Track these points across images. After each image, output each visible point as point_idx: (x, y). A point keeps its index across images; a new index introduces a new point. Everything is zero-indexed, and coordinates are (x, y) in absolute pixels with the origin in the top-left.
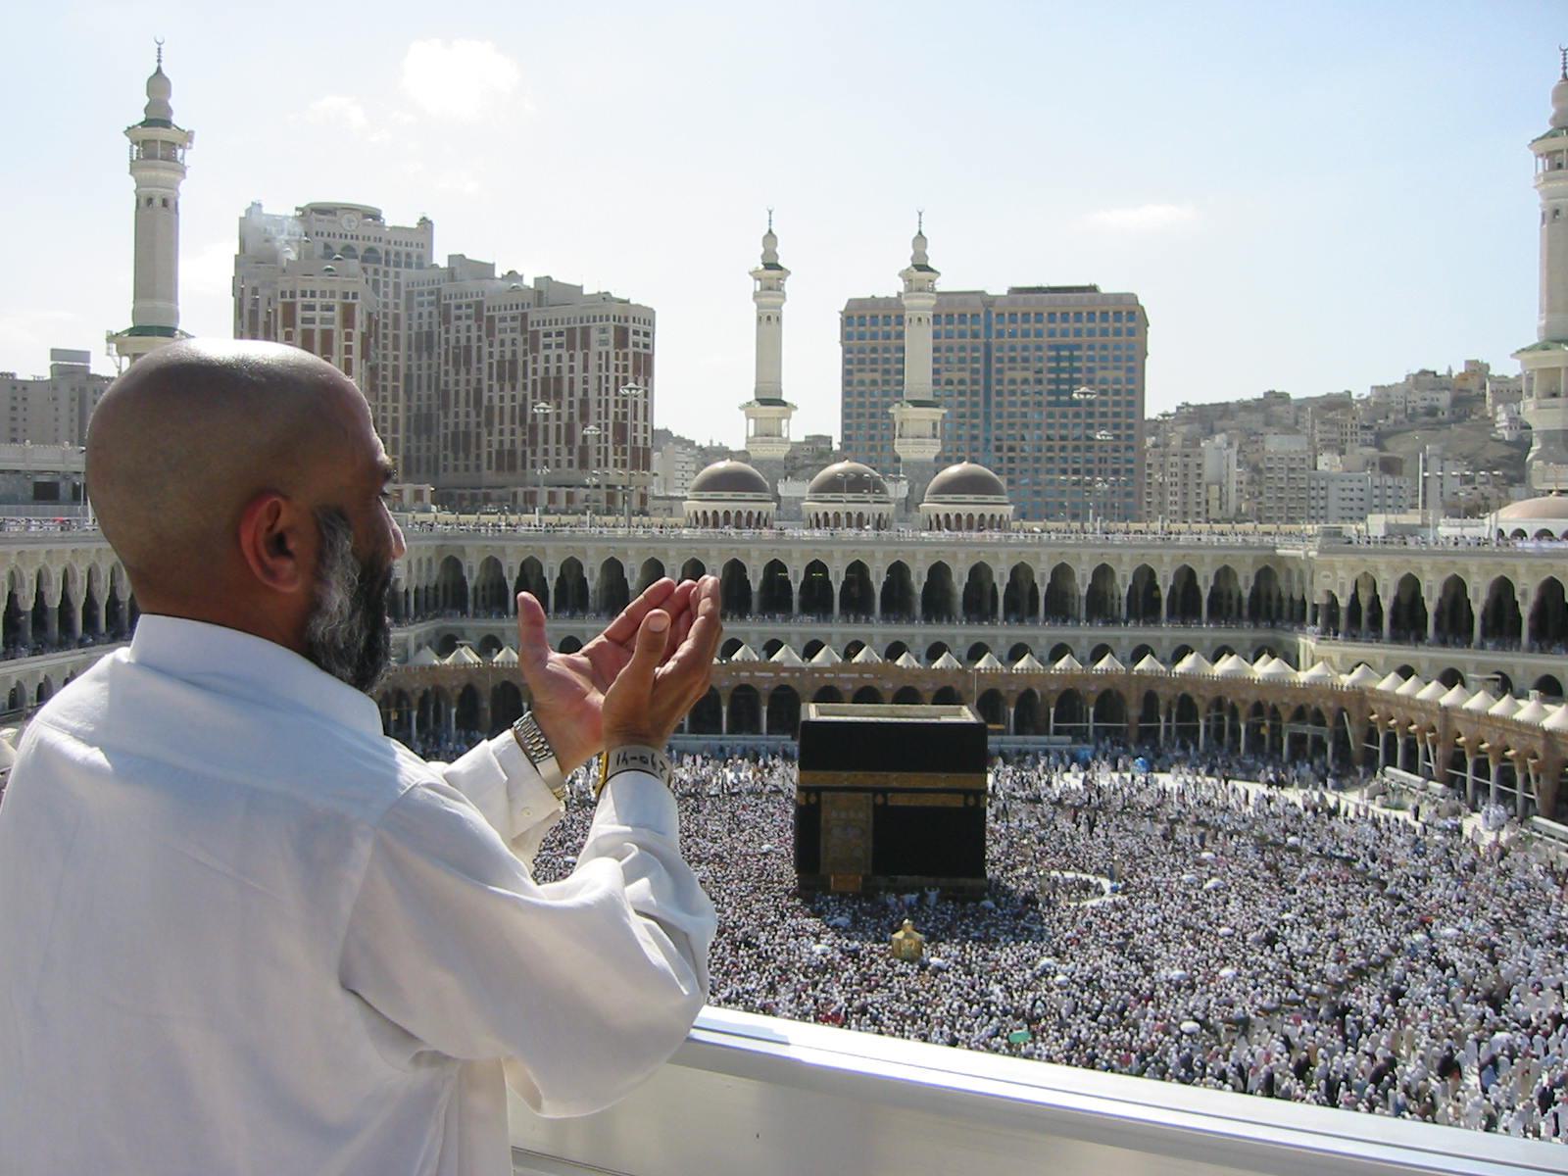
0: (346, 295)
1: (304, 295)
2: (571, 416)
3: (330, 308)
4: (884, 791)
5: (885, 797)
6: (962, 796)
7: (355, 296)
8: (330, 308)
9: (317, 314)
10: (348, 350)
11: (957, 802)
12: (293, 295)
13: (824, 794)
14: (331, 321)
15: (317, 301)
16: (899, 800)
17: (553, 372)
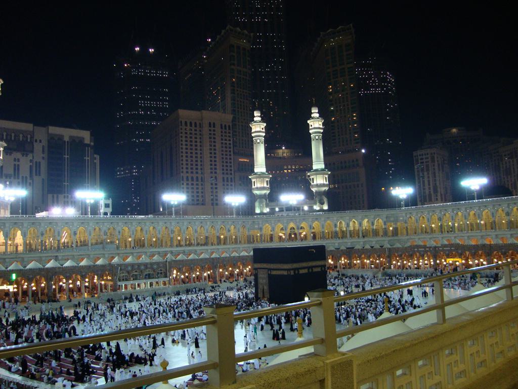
0: (432, 154)
1: (420, 155)
2: (515, 179)
3: (427, 158)
4: (270, 269)
5: (271, 272)
6: (287, 271)
7: (434, 153)
8: (427, 158)
9: (424, 160)
10: (434, 169)
11: (285, 273)
12: (417, 156)
13: (258, 270)
14: (428, 162)
15: (424, 157)
16: (274, 273)
17: (508, 167)
